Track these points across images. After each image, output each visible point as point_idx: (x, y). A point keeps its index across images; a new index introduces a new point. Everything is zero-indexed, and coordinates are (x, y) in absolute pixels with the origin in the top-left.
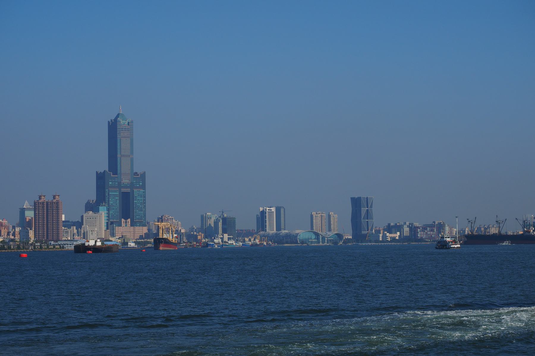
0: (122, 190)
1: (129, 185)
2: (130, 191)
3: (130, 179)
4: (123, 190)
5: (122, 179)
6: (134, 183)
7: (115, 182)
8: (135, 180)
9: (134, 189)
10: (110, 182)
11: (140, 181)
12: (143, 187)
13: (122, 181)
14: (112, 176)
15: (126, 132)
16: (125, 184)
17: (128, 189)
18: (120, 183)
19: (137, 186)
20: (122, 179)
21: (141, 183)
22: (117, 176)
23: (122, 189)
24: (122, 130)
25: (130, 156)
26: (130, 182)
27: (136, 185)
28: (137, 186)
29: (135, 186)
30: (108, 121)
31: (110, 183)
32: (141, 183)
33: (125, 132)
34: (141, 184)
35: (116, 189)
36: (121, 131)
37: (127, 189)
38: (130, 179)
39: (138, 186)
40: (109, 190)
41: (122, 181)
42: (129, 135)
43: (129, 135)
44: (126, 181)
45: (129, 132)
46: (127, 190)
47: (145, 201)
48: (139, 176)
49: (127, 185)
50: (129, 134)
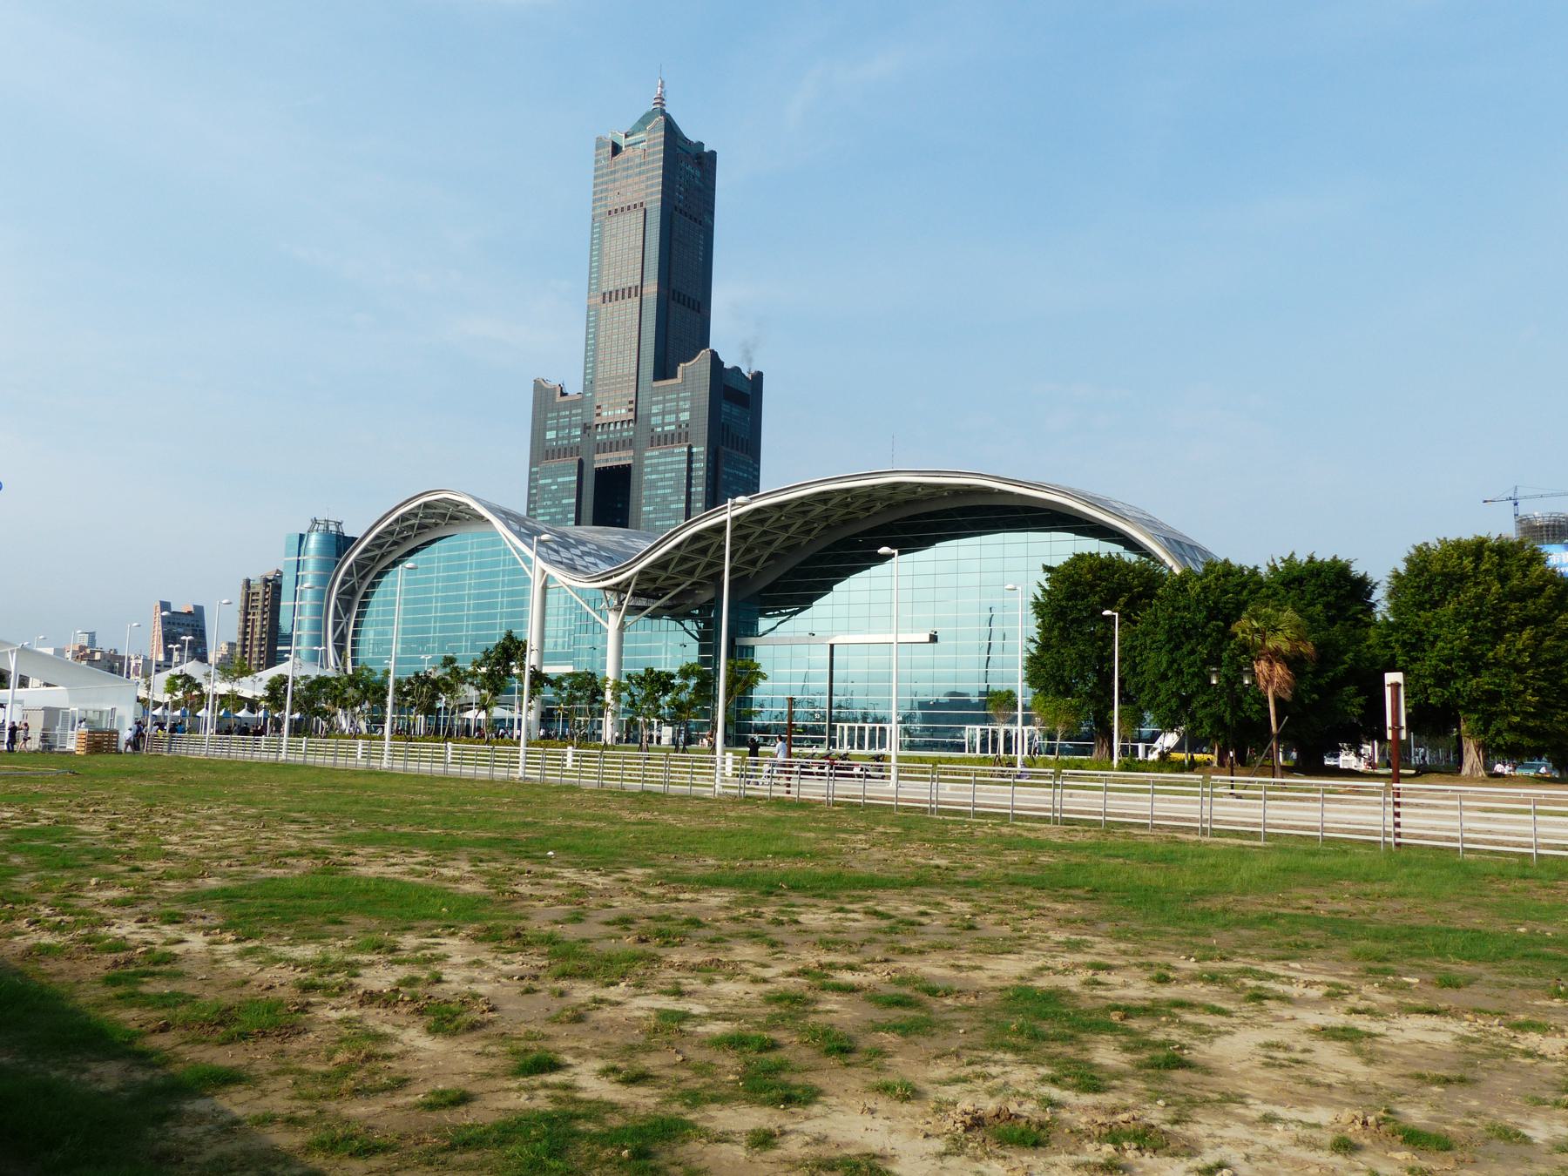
0: (599, 461)
2: (630, 462)
5: (599, 407)
6: (653, 419)
7: (570, 426)
8: (657, 403)
10: (551, 430)
11: (681, 403)
17: (623, 454)
23: (597, 457)
27: (663, 425)
28: (666, 428)
29: (659, 429)
31: (551, 435)
32: (684, 410)
37: (616, 455)
38: (631, 402)
39: (673, 427)
41: (598, 415)
46: (620, 459)
49: (621, 431)
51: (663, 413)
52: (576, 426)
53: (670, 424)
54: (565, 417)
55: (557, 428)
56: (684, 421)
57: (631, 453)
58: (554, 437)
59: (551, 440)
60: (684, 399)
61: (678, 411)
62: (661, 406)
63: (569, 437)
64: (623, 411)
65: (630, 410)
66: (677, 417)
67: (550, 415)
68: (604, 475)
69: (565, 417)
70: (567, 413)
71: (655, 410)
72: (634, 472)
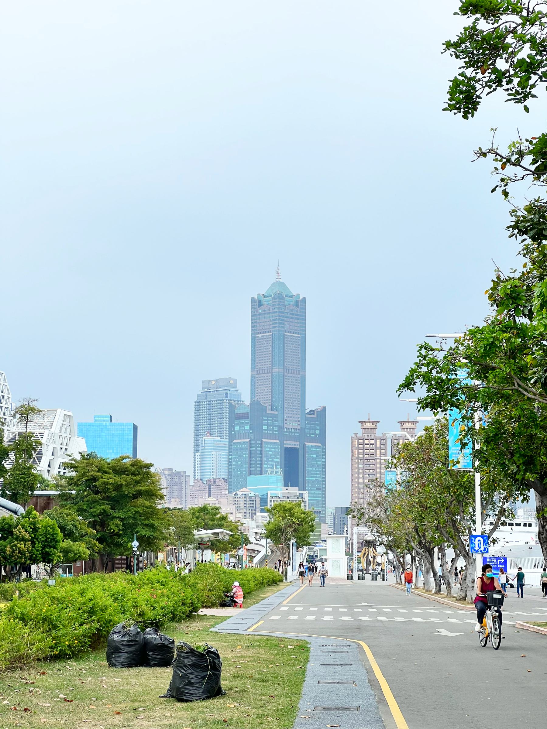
0: (285, 444)
1: (297, 433)
2: (298, 447)
3: (299, 421)
4: (287, 444)
5: (286, 420)
7: (273, 425)
8: (308, 424)
9: (306, 443)
11: (316, 426)
12: (322, 438)
13: (286, 423)
14: (268, 412)
15: (293, 320)
16: (290, 430)
18: (281, 428)
19: (311, 436)
20: (286, 420)
21: (319, 431)
22: (276, 413)
23: (285, 442)
24: (287, 317)
25: (301, 373)
26: (299, 427)
27: (310, 434)
28: (311, 436)
29: (308, 435)
30: (253, 298)
31: (265, 427)
32: (318, 429)
33: (291, 320)
34: (318, 432)
35: (275, 441)
36: (286, 319)
37: (293, 443)
38: (299, 421)
39: (314, 436)
40: (262, 441)
41: (286, 423)
42: (299, 329)
43: (299, 329)
44: (292, 425)
45: (299, 321)
46: (294, 445)
47: (325, 468)
48: (315, 416)
49: (294, 432)
50: (299, 325)
51: (310, 429)
52: (276, 426)
53: (312, 434)
54: (270, 420)
55: (268, 425)
56: (317, 434)
57: (298, 443)
58: (266, 429)
59: (265, 430)
60: (318, 425)
61: (316, 429)
62: (309, 426)
63: (273, 429)
64: (297, 424)
65: (299, 425)
66: (315, 432)
67: (264, 418)
68: (287, 449)
69: (270, 420)
70: (271, 419)
71: (307, 426)
72: (301, 452)
